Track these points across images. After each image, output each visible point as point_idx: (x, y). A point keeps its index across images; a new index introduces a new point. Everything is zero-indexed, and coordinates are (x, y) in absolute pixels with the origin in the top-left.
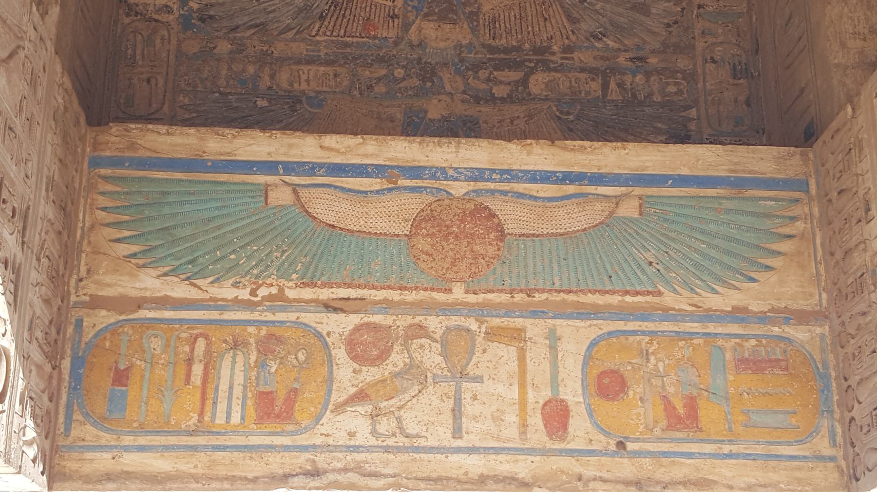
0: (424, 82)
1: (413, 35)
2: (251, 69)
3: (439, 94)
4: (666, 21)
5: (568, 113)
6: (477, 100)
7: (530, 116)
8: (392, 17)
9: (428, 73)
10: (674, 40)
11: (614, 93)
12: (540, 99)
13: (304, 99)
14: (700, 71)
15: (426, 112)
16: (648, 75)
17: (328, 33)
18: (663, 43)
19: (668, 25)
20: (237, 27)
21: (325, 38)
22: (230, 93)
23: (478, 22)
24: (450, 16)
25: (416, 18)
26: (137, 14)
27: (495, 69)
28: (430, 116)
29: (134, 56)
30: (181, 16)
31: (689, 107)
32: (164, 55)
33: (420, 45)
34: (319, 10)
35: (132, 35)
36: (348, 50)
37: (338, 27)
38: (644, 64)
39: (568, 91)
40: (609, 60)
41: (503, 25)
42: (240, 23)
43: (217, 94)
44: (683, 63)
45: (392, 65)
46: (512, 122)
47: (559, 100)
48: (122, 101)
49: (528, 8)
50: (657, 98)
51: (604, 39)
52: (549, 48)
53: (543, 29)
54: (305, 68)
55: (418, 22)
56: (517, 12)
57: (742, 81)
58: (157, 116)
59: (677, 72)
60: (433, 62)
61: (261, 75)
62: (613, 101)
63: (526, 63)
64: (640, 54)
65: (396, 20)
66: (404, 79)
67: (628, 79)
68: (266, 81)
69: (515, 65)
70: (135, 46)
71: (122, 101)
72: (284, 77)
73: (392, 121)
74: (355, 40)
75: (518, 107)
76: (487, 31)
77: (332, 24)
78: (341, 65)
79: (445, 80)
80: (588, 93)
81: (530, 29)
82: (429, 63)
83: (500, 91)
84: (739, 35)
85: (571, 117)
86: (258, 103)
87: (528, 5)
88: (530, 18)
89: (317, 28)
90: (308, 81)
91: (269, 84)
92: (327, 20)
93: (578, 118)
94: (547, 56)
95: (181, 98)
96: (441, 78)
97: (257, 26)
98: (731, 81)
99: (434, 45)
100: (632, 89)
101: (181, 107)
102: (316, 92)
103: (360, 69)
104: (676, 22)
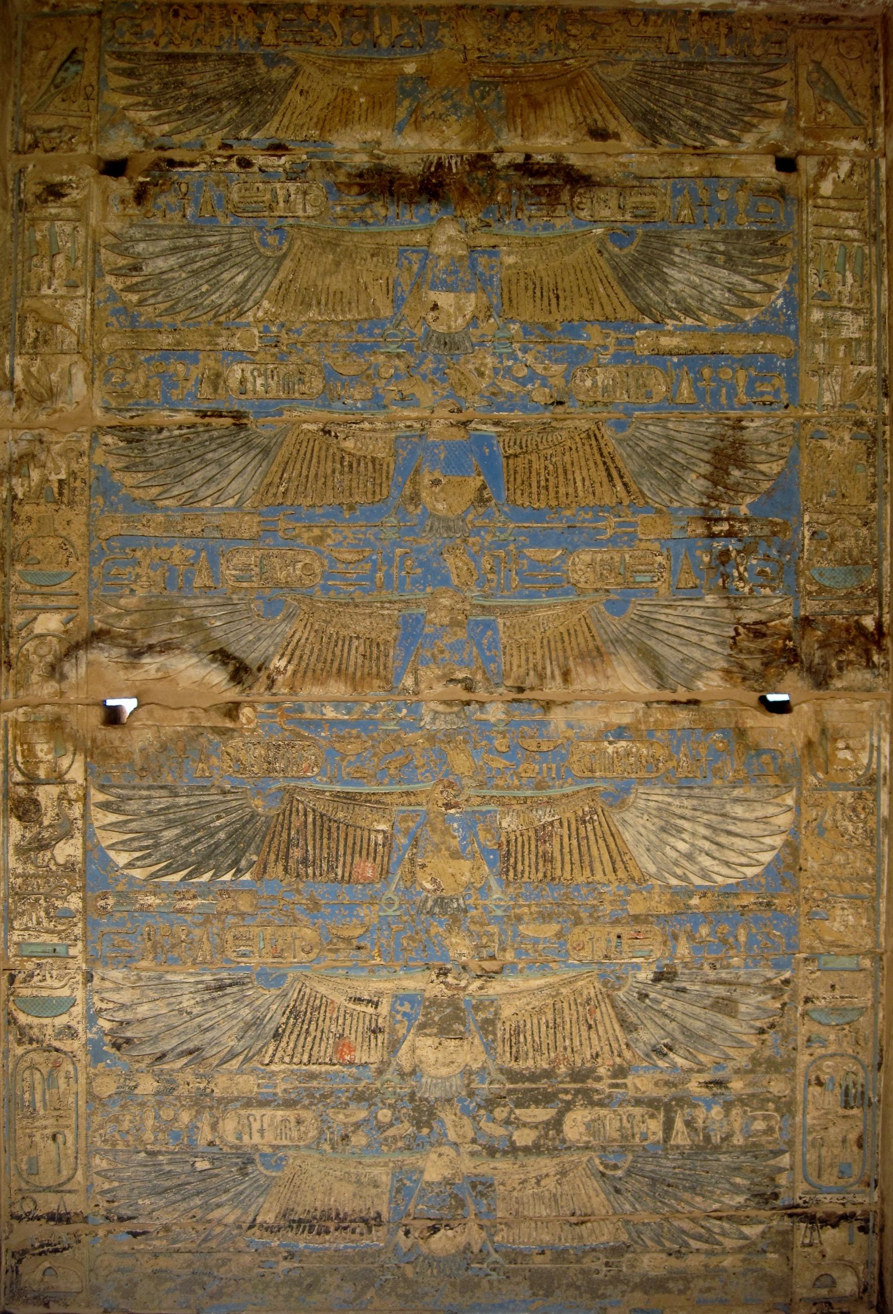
0: (419, 1128)
1: (404, 1058)
2: (185, 1117)
3: (440, 1144)
4: (758, 1024)
5: (616, 1167)
6: (492, 1152)
7: (563, 1173)
8: (374, 1032)
9: (424, 1114)
10: (767, 1053)
11: (681, 1137)
12: (578, 1148)
13: (257, 1157)
14: (799, 1097)
15: (422, 1172)
16: (728, 1106)
17: (287, 1059)
18: (753, 1059)
19: (762, 1031)
20: (164, 1055)
21: (283, 1067)
22: (159, 1152)
23: (495, 1034)
24: (456, 1026)
25: (408, 1031)
26: (31, 1041)
27: (518, 1105)
28: (427, 1177)
29: (33, 1102)
30: (89, 1041)
31: (777, 1153)
32: (71, 1099)
33: (413, 1072)
34: (273, 1025)
35: (27, 1074)
36: (315, 1084)
37: (300, 1049)
38: (723, 1090)
39: (616, 1135)
40: (675, 1085)
41: (529, 1039)
42: (168, 1048)
43: (143, 1155)
44: (777, 1086)
45: (375, 1104)
46: (538, 1183)
47: (604, 1148)
48: (24, 1167)
49: (566, 1011)
50: (738, 1140)
51: (671, 1055)
52: (592, 1070)
53: (586, 1043)
54: (257, 1112)
55: (410, 1037)
56: (550, 1017)
57: (855, 1111)
58: (67, 1187)
59: (768, 1100)
60: (432, 1098)
61: (199, 1125)
62: (678, 1147)
63: (561, 1096)
64: (719, 1075)
65: (380, 1036)
66: (391, 1125)
67: (700, 1114)
68: (205, 1135)
69: (546, 1099)
70: (32, 1087)
71: (24, 1167)
72: (229, 1127)
73: (376, 1186)
74: (324, 1068)
75: (547, 1161)
76: (507, 1049)
77: (292, 1045)
78: (305, 1107)
79: (449, 1124)
80: (644, 1137)
81: (568, 1043)
82: (426, 1100)
83: (524, 1137)
84: (857, 1043)
85: (619, 1173)
86: (197, 1165)
87: (565, 1005)
88: (568, 1026)
89: (270, 1052)
90: (261, 1131)
91: (210, 1138)
92: (285, 1039)
93: (629, 1173)
94: (590, 1084)
95: (97, 1160)
96: (442, 1121)
97: (190, 1052)
98: (841, 1111)
99: (433, 1072)
100: (705, 1128)
101: (98, 1173)
102: (272, 1146)
103: (331, 1112)
104: (772, 1026)
